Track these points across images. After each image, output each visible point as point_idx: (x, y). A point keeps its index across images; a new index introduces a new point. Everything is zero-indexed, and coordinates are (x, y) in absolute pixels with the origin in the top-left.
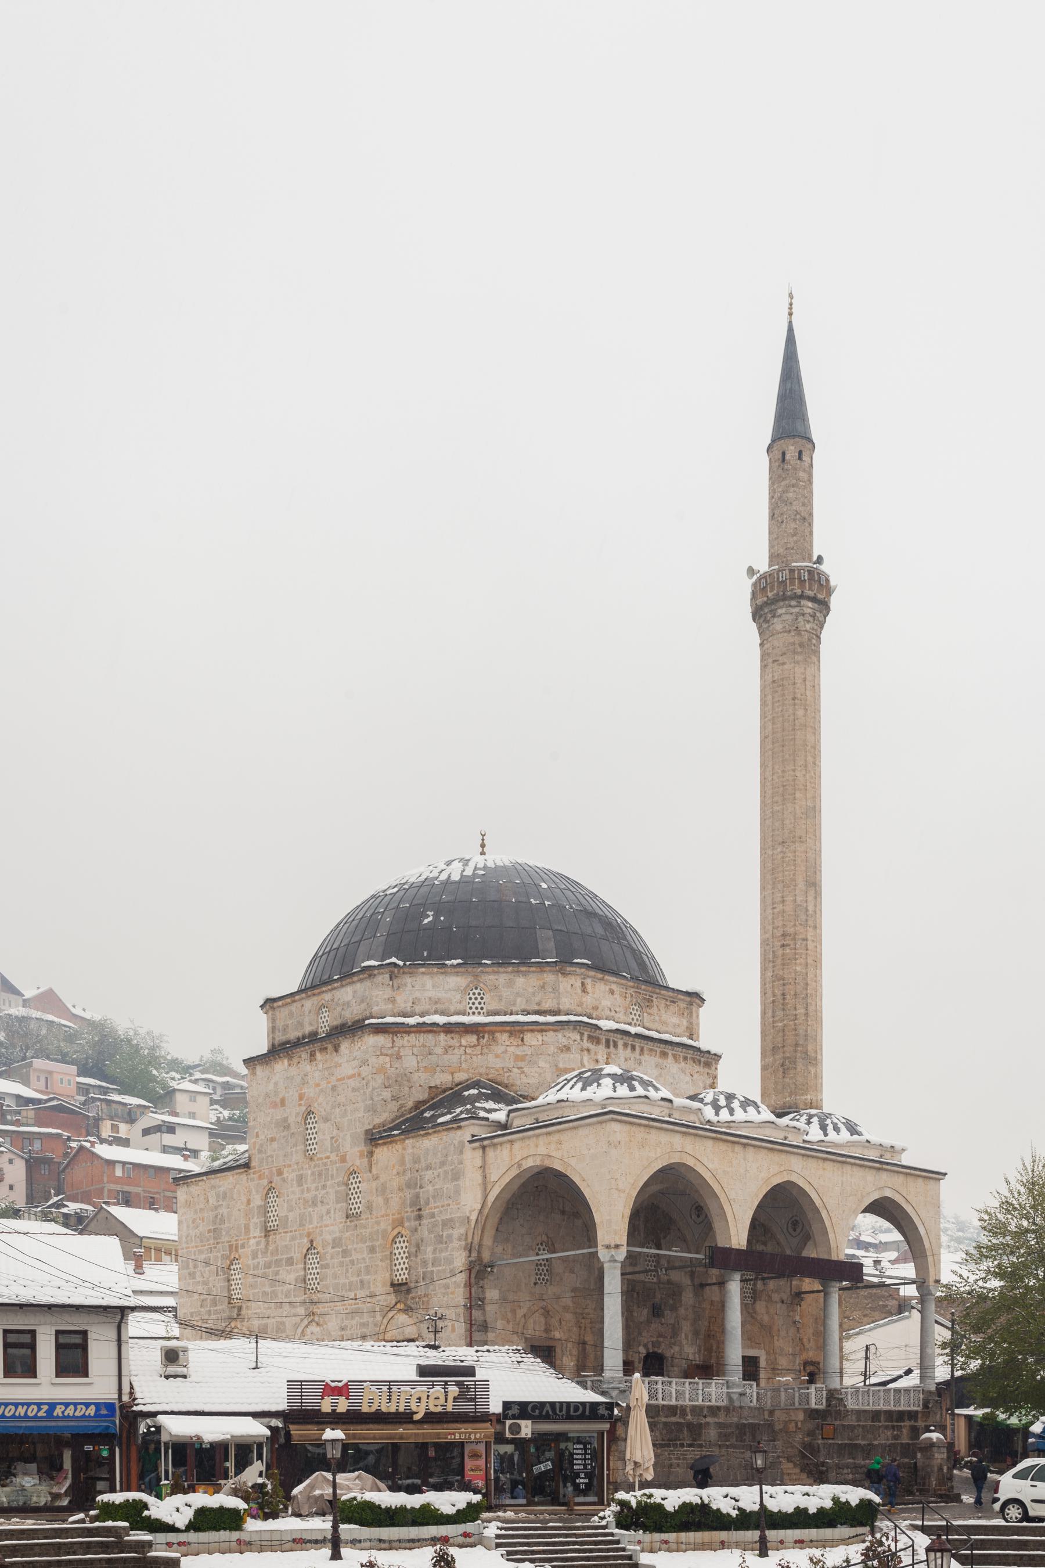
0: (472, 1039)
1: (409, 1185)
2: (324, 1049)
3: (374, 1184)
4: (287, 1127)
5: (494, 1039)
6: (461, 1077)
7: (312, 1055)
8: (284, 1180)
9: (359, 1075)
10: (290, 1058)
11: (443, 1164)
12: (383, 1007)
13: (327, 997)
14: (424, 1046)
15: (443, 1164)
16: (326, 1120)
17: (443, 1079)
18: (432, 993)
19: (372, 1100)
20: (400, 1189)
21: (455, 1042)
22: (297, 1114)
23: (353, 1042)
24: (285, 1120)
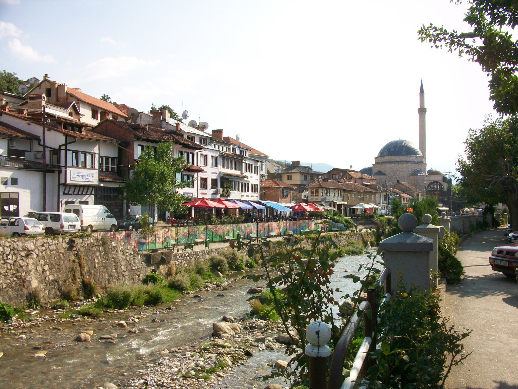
17: (415, 169)
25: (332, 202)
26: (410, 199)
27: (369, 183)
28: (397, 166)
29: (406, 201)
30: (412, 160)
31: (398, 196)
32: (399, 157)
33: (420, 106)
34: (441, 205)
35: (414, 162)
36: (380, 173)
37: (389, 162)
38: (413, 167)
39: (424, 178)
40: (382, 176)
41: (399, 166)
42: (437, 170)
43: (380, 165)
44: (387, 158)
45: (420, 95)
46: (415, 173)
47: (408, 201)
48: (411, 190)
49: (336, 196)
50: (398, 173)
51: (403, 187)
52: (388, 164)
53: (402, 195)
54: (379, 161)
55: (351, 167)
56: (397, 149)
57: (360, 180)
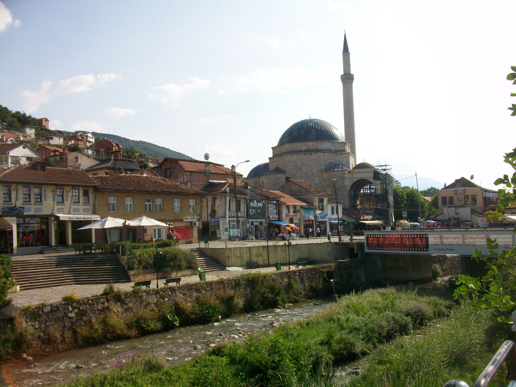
2: (307, 154)
3: (322, 179)
4: (298, 167)
5: (338, 155)
6: (334, 161)
7: (304, 155)
10: (298, 154)
11: (340, 177)
12: (320, 147)
13: (305, 144)
17: (331, 161)
19: (321, 163)
22: (300, 165)
25: (52, 215)
26: (302, 207)
28: (302, 159)
30: (325, 148)
31: (275, 202)
32: (305, 144)
33: (344, 71)
34: (370, 217)
35: (329, 151)
36: (278, 170)
37: (290, 152)
38: (326, 158)
39: (344, 174)
40: (279, 175)
41: (305, 158)
42: (365, 162)
43: (278, 158)
44: (287, 147)
45: (344, 56)
46: (331, 167)
47: (299, 211)
48: (308, 191)
49: (68, 203)
50: (304, 167)
51: (296, 188)
52: (288, 155)
53: (282, 200)
55: (207, 157)
56: (302, 131)
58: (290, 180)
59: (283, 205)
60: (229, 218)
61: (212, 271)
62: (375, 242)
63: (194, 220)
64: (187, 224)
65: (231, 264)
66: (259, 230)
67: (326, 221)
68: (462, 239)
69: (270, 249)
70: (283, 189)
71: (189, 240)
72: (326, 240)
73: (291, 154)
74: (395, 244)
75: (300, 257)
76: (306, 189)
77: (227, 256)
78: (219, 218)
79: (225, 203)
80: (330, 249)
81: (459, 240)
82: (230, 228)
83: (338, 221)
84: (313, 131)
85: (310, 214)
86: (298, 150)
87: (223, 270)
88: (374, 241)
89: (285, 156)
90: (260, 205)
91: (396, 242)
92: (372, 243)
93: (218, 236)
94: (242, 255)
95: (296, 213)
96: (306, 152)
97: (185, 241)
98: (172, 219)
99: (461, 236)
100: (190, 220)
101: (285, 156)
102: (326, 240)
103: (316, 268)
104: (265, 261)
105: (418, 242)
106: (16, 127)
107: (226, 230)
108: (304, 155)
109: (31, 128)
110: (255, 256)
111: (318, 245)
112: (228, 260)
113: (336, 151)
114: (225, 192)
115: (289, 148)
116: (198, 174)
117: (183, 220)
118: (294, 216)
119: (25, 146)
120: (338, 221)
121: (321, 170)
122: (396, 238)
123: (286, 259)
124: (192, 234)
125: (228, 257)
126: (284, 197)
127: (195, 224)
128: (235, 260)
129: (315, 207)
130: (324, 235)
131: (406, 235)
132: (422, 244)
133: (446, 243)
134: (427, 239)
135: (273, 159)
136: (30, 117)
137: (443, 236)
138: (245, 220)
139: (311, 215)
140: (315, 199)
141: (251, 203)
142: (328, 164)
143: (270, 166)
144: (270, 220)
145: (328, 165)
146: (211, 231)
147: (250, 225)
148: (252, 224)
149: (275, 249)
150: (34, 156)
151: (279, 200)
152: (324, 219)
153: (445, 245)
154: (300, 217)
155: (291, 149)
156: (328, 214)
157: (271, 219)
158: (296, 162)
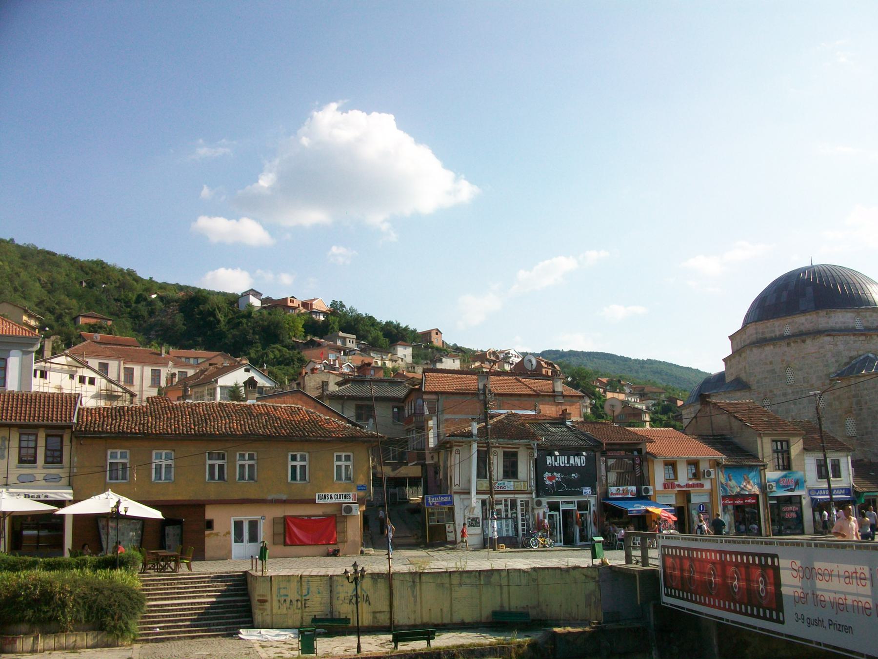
0: (863, 338)
1: (854, 396)
2: (795, 342)
4: (776, 373)
6: (861, 353)
7: (789, 344)
8: (774, 395)
9: (819, 352)
10: (774, 345)
14: (845, 341)
15: (874, 388)
16: (801, 370)
17: (854, 354)
18: (842, 320)
19: (827, 361)
20: (849, 398)
21: (857, 339)
23: (814, 339)
24: (774, 370)
26: (717, 464)
27: (533, 413)
29: (696, 476)
30: (838, 326)
32: (789, 319)
35: (850, 331)
36: (740, 385)
38: (841, 347)
41: (791, 351)
43: (737, 357)
44: (751, 329)
51: (721, 420)
52: (754, 350)
53: (649, 448)
54: (740, 347)
57: (475, 399)
58: (708, 402)
59: (653, 461)
60: (477, 493)
61: (193, 637)
62: (677, 573)
63: (347, 501)
64: (329, 511)
65: (268, 620)
66: (577, 523)
67: (800, 496)
68: (868, 583)
69: (396, 583)
70: (697, 422)
71: (331, 548)
72: (581, 559)
73: (760, 347)
74: (710, 582)
75: (502, 606)
76: (741, 420)
77: (257, 598)
78: (451, 496)
79: (470, 457)
80: (592, 586)
81: (861, 590)
82: (485, 518)
83: (828, 497)
84: (810, 290)
85: (745, 479)
86: (776, 336)
87: (230, 635)
88: (674, 569)
89: (748, 352)
90: (579, 461)
91: (713, 579)
92: (671, 575)
93: (450, 537)
94: (307, 598)
95: (699, 479)
96: (793, 339)
97: (322, 549)
98: (284, 497)
99: (866, 571)
100: (333, 501)
101: (748, 352)
102: (581, 559)
103: (439, 654)
104: (378, 615)
105: (758, 582)
106: (381, 347)
107: (474, 522)
108: (789, 344)
109: (405, 346)
110: (347, 601)
111: (558, 572)
112: (260, 609)
113: (868, 329)
114: (470, 434)
115: (756, 333)
116: (457, 398)
117: (313, 501)
118: (692, 486)
119: (248, 367)
120: (828, 497)
121: (829, 374)
122: (714, 563)
123: (451, 611)
124: (345, 532)
125: (259, 601)
126: (651, 441)
127: (349, 509)
128: (284, 611)
129: (763, 461)
130: (798, 531)
131: (731, 553)
132: (766, 589)
133: (828, 597)
134: (776, 569)
135: (730, 360)
136: (406, 329)
137: (817, 565)
138: (532, 498)
139: (749, 482)
140: (762, 441)
141: (548, 457)
142: (845, 360)
143: (726, 375)
144: (610, 496)
145: (846, 364)
146: (430, 527)
147: (547, 510)
148: (554, 507)
149: (414, 582)
150: (268, 385)
151: (641, 449)
152: (792, 490)
153: (822, 604)
154: (712, 489)
155: (760, 336)
156: (808, 480)
157: (612, 494)
158: (771, 363)
